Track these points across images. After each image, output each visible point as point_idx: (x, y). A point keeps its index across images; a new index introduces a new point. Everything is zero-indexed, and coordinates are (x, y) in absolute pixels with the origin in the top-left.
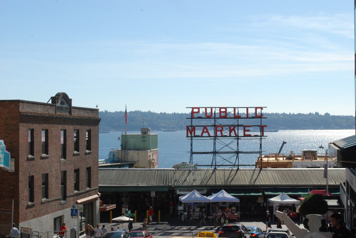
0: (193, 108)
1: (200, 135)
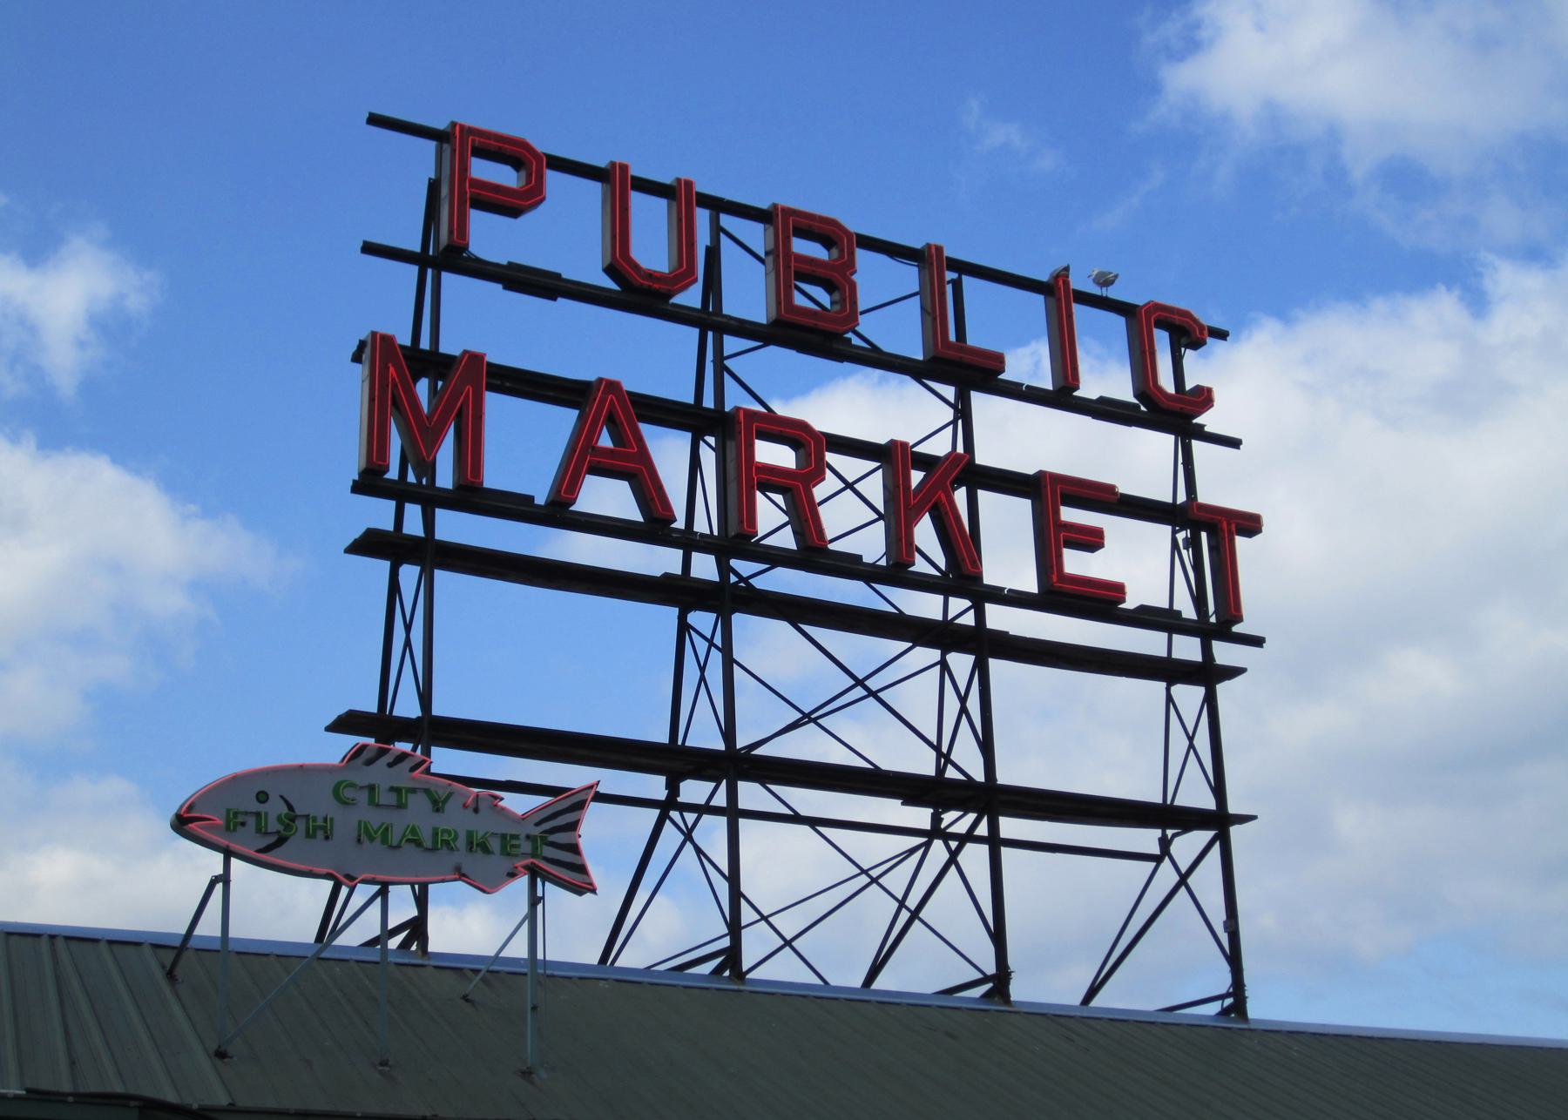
1: (540, 500)
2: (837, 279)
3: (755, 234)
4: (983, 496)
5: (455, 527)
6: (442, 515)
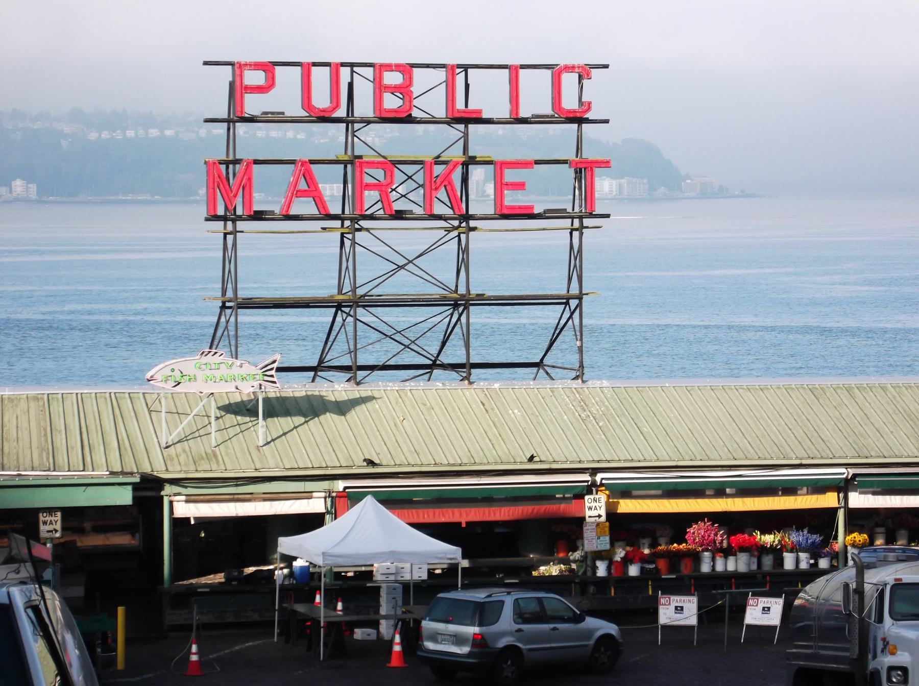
0: (238, 68)
2: (404, 90)
3: (369, 72)
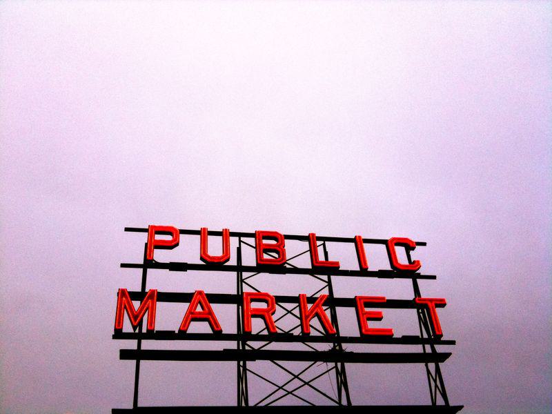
1: (177, 332)
2: (280, 249)
3: (252, 241)
4: (338, 309)
5: (148, 345)
6: (143, 341)
